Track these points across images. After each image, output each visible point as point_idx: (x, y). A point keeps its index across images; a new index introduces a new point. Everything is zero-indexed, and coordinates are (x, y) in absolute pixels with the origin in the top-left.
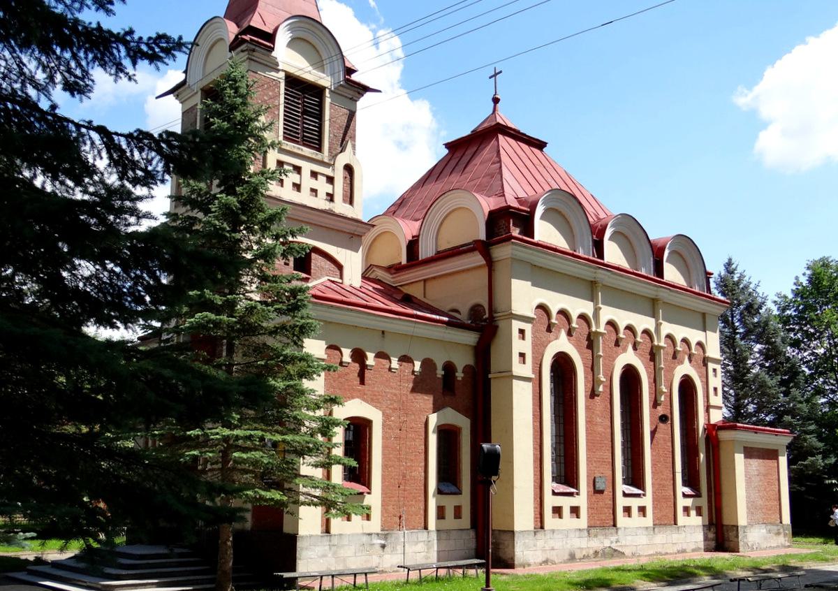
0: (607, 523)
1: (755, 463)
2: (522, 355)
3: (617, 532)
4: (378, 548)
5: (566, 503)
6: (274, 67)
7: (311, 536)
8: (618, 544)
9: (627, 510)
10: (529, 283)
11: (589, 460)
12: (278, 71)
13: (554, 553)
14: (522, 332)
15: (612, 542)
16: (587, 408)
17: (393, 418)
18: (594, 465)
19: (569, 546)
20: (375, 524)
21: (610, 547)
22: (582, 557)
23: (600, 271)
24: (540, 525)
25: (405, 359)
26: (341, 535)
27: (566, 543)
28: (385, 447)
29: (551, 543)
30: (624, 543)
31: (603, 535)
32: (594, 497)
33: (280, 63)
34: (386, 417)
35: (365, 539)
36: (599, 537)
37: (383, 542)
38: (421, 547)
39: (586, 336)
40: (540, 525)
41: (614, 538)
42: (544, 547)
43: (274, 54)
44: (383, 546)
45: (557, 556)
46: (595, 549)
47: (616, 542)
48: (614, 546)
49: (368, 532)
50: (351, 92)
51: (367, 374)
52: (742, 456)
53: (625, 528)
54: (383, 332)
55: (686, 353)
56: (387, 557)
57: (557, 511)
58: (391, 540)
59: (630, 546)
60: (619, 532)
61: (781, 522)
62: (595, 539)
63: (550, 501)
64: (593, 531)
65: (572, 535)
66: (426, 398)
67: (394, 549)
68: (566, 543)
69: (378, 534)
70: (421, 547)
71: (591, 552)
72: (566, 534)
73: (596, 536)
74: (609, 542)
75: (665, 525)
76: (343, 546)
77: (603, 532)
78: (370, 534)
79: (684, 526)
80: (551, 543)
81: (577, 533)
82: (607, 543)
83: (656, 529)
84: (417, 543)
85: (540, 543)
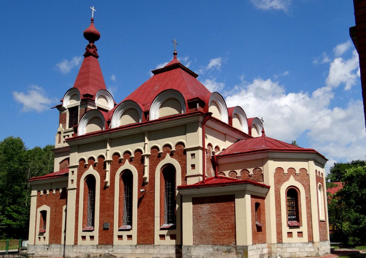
0: (110, 243)
1: (205, 208)
2: (72, 181)
3: (113, 247)
4: (46, 249)
5: (88, 235)
6: (65, 109)
7: (31, 245)
8: (113, 252)
9: (120, 237)
10: (77, 152)
11: (101, 217)
12: (66, 109)
13: (81, 254)
14: (73, 172)
15: (109, 251)
16: (101, 194)
17: (54, 209)
18: (104, 218)
19: (87, 252)
20: (47, 242)
21: (108, 253)
22: (93, 256)
23: (103, 135)
24: (76, 243)
25: (57, 190)
26: (37, 245)
27: (86, 250)
28: (51, 218)
29: (79, 250)
30: (116, 252)
31: (105, 248)
32: (104, 232)
33: (65, 107)
34: (52, 209)
35: (43, 246)
36: (102, 249)
37: (48, 248)
38: (58, 250)
39: (103, 164)
40: (76, 243)
41: (111, 250)
42: (76, 251)
43: (63, 106)
44: (48, 249)
45: (82, 255)
46: (100, 254)
47: (112, 251)
48: (110, 253)
49: (44, 244)
50: (84, 102)
51: (48, 197)
52: (190, 204)
53: (118, 245)
54: (51, 183)
55: (168, 152)
56: (48, 252)
57: (84, 238)
58: (50, 247)
59: (120, 253)
60: (114, 247)
61: (236, 244)
62: (100, 249)
63: (81, 233)
64: (99, 246)
65: (88, 247)
66: (63, 201)
67: (51, 250)
68: (86, 250)
69: (46, 245)
70: (58, 250)
71: (98, 255)
72: (87, 247)
73: (101, 248)
74: (108, 251)
75: (147, 244)
76: (37, 248)
77: (105, 247)
78: (44, 245)
79: (159, 245)
80: (79, 250)
81: (92, 247)
82: (107, 251)
83: (138, 247)
84: (57, 248)
85: (75, 250)
